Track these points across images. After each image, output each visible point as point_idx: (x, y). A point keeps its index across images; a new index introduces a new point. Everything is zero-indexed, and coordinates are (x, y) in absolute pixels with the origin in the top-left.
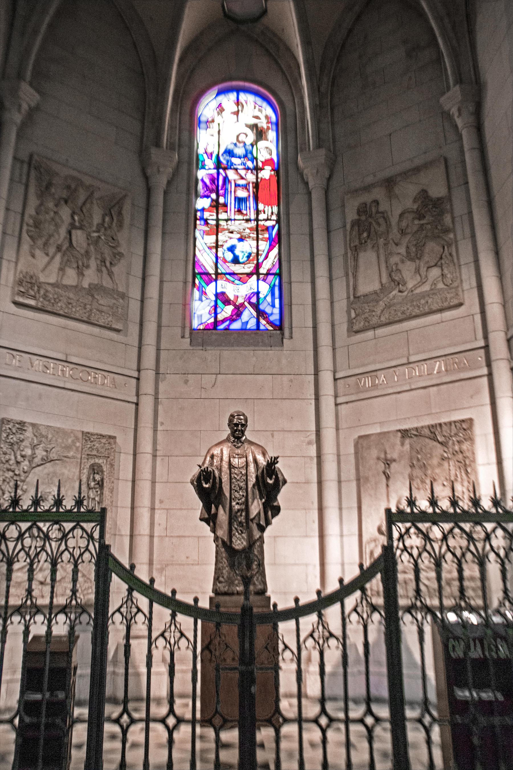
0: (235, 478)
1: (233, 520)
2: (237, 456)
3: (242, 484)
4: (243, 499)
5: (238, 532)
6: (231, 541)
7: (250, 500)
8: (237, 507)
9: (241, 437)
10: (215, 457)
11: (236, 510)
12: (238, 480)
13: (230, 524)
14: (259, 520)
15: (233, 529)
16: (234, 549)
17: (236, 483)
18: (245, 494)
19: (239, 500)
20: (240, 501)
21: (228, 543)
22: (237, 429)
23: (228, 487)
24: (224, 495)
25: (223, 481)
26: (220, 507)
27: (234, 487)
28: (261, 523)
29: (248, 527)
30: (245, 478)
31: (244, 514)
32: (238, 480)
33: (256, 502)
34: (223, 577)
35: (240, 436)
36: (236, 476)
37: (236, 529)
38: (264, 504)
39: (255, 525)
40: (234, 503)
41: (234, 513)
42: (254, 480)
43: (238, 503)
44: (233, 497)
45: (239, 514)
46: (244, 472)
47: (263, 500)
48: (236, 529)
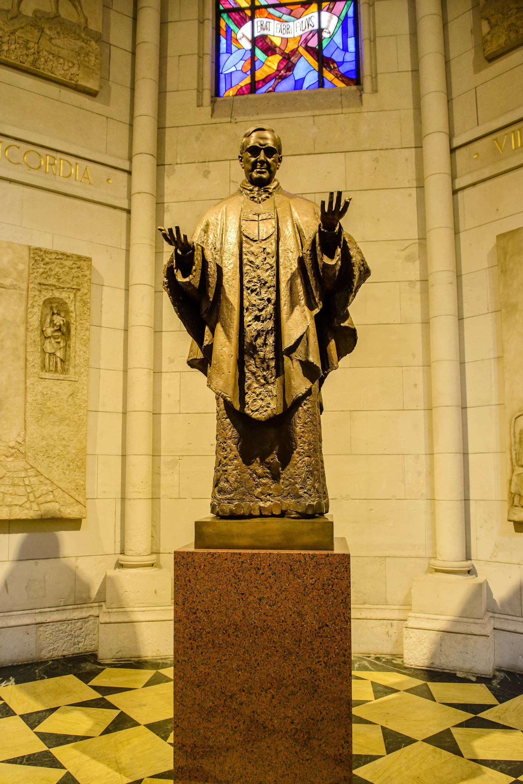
0: (251, 262)
1: (246, 358)
2: (256, 217)
3: (267, 276)
4: (270, 308)
5: (258, 381)
6: (243, 403)
7: (285, 309)
8: (257, 326)
9: (269, 181)
10: (211, 227)
11: (255, 333)
12: (258, 267)
13: (241, 364)
14: (307, 354)
15: (248, 375)
16: (248, 417)
17: (253, 274)
18: (273, 297)
19: (261, 310)
20: (263, 313)
21: (237, 407)
22: (256, 162)
23: (236, 284)
24: (227, 299)
25: (225, 271)
26: (219, 327)
27: (249, 282)
28: (311, 359)
29: (280, 370)
30: (272, 261)
31: (271, 340)
32: (258, 267)
33: (297, 311)
34: (227, 481)
35: (264, 176)
36: (252, 258)
37: (254, 373)
38: (317, 319)
39: (297, 364)
40: (248, 318)
41: (248, 340)
42: (295, 266)
43: (257, 318)
44: (246, 304)
45: (260, 341)
46: (271, 248)
47: (317, 311)
48: (254, 373)
